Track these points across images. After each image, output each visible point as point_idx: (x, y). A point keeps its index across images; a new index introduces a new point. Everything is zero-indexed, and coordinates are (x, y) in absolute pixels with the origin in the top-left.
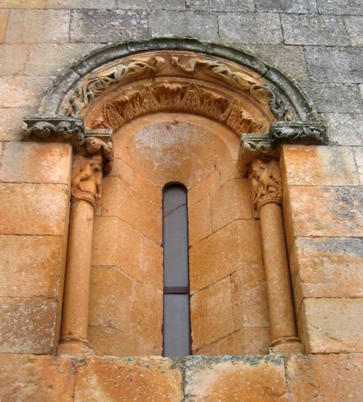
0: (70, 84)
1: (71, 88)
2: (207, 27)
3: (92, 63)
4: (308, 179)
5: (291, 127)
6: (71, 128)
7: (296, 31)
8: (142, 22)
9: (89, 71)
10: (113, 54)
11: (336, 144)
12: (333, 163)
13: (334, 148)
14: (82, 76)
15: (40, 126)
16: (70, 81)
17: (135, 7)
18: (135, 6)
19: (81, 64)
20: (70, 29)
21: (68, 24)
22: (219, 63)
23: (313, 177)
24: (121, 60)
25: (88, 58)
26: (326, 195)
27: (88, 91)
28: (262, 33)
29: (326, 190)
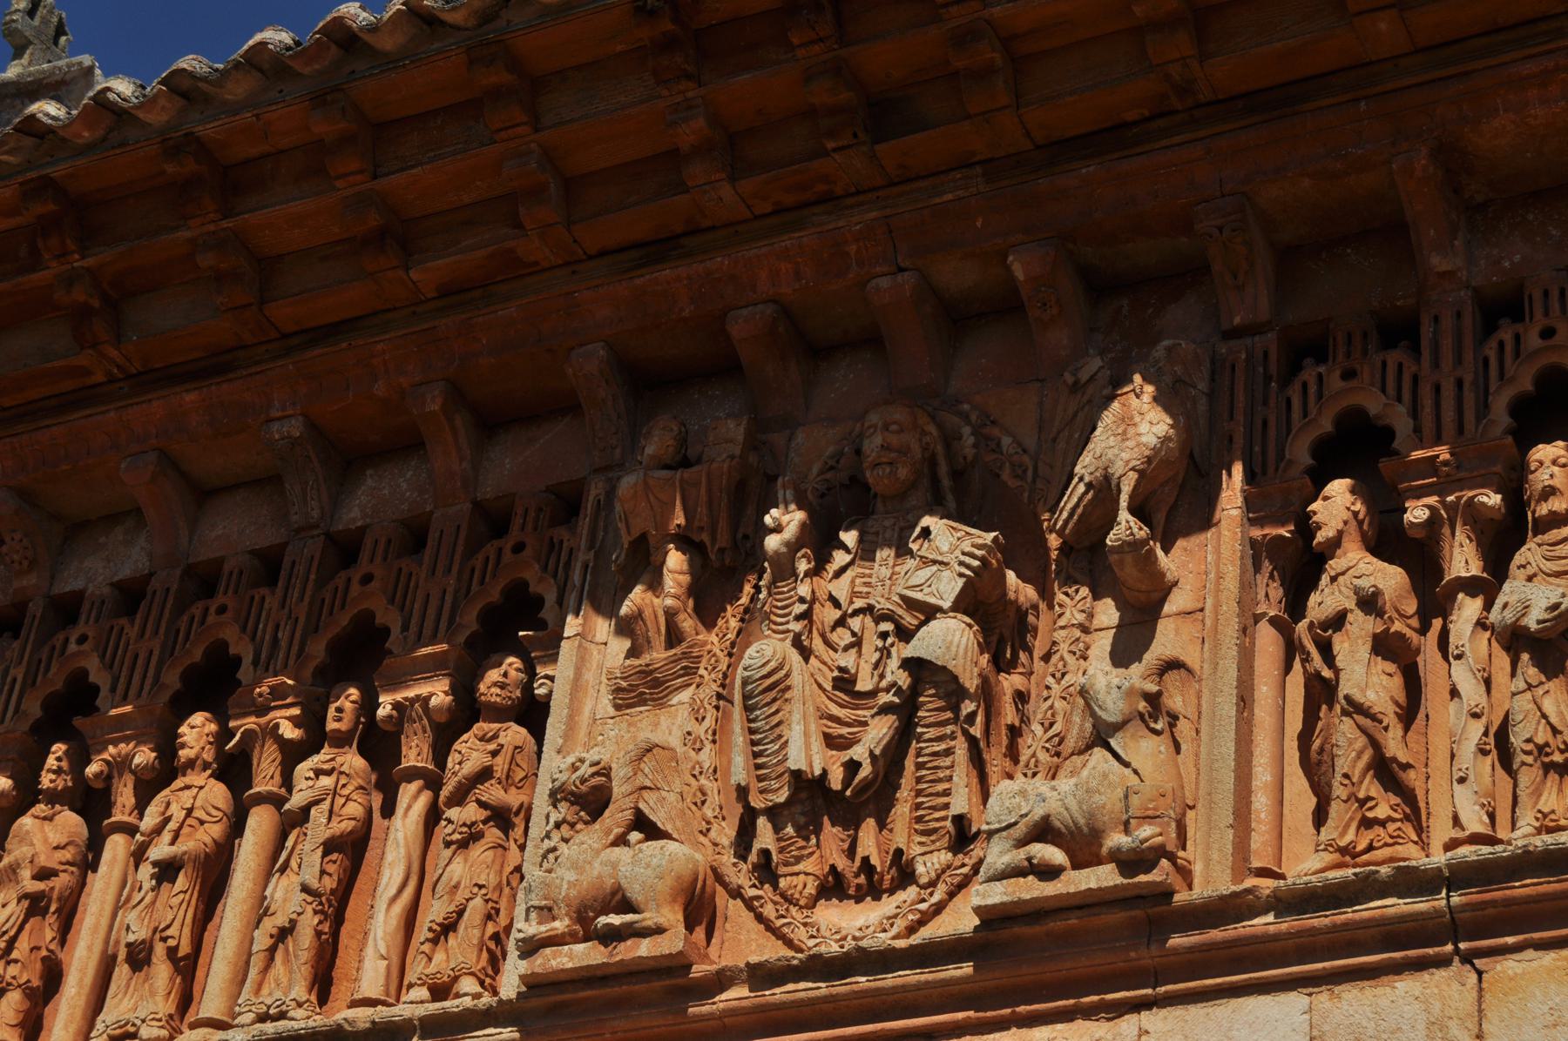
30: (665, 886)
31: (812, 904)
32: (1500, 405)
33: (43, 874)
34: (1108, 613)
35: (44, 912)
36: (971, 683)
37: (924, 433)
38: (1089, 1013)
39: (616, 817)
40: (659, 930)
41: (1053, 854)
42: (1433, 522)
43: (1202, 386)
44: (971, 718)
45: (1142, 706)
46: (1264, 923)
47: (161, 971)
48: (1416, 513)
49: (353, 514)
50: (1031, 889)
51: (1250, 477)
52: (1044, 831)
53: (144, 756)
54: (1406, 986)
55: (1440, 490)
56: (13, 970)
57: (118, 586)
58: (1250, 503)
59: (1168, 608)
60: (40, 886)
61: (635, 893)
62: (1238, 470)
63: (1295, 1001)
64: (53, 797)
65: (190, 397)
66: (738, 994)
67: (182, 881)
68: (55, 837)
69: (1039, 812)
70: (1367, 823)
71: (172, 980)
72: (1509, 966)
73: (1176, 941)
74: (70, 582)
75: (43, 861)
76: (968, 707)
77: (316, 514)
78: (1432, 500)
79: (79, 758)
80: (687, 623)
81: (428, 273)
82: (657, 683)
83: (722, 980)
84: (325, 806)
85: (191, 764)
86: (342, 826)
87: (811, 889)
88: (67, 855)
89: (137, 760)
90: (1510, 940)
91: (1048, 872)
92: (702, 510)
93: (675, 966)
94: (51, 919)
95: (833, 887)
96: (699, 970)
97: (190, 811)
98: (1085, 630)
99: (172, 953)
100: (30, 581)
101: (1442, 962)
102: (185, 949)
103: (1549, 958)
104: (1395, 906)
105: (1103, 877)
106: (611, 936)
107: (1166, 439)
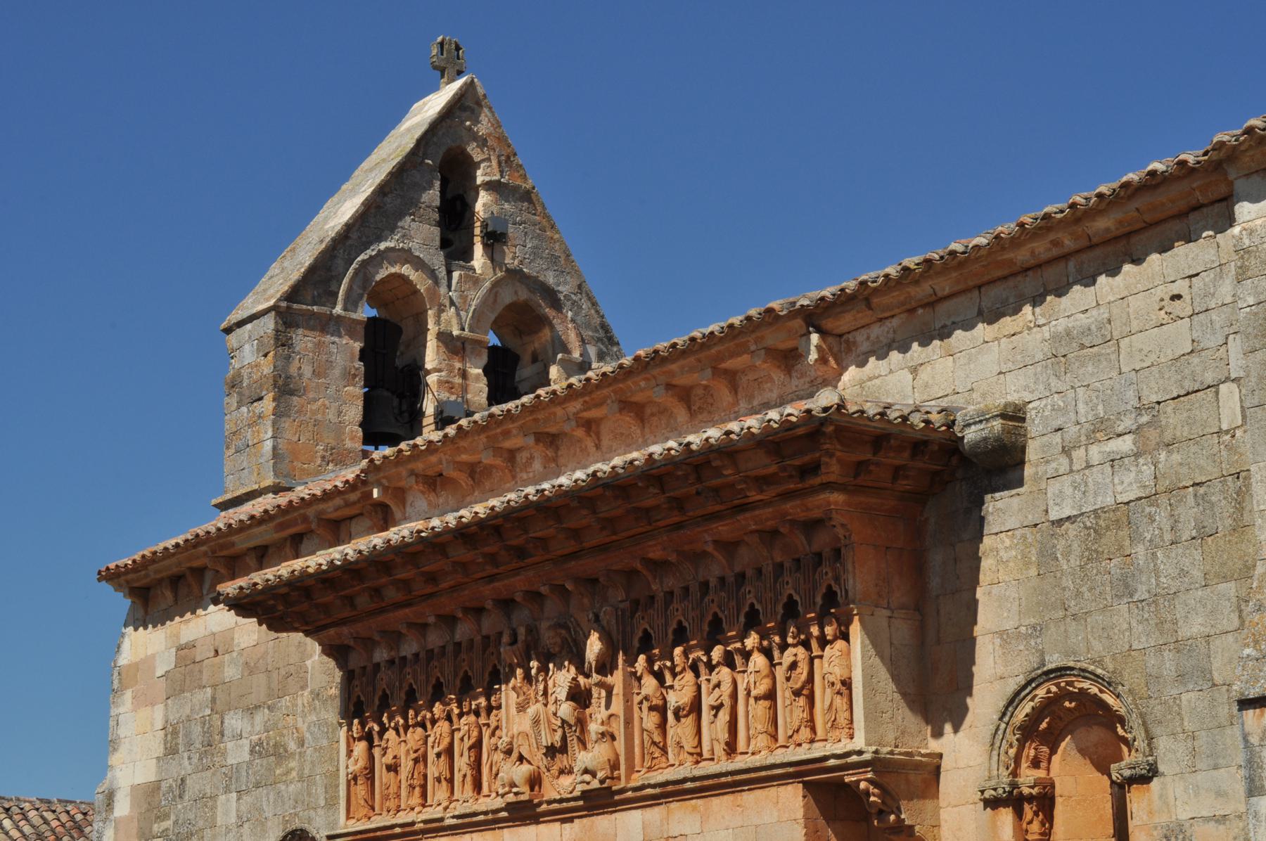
0: (1001, 737)
1: (1002, 739)
2: (1080, 638)
3: (1010, 709)
4: (1145, 818)
5: (1129, 768)
6: (1005, 792)
7: (1140, 628)
8: (1039, 640)
9: (1011, 716)
10: (1023, 694)
11: (1163, 774)
12: (1161, 796)
13: (1162, 779)
14: (1007, 724)
15: (987, 795)
16: (1000, 732)
17: (1033, 621)
18: (1032, 619)
19: (1004, 714)
20: (995, 663)
21: (992, 655)
22: (1091, 684)
23: (1148, 816)
24: (1029, 697)
25: (1007, 708)
26: (1155, 833)
27: (1014, 735)
28: (1116, 637)
29: (1156, 828)
30: (523, 781)
31: (558, 777)
32: (670, 631)
33: (416, 751)
34: (603, 693)
35: (419, 761)
36: (572, 722)
37: (561, 634)
38: (607, 813)
39: (515, 755)
40: (523, 793)
41: (587, 777)
42: (660, 667)
43: (614, 621)
44: (575, 731)
45: (600, 736)
46: (630, 794)
47: (444, 783)
48: (656, 668)
49: (458, 638)
50: (586, 787)
51: (625, 654)
52: (586, 771)
53: (429, 715)
54: (657, 809)
55: (660, 659)
56: (415, 781)
57: (413, 654)
58: (625, 661)
59: (614, 692)
60: (416, 755)
61: (517, 783)
62: (621, 652)
63: (639, 811)
64: (414, 726)
65: (407, 610)
66: (544, 807)
67: (443, 758)
68: (417, 738)
69: (584, 767)
70: (654, 758)
71: (447, 786)
72: (673, 805)
73: (617, 798)
74: (403, 654)
75: (414, 748)
76: (574, 728)
77: (448, 638)
78: (658, 663)
79: (416, 716)
80: (525, 689)
81: (444, 585)
82: (522, 707)
83: (540, 804)
84: (467, 736)
85: (439, 719)
86: (473, 740)
87: (557, 774)
88: (421, 742)
89: (427, 717)
90: (671, 799)
91: (588, 783)
92: (519, 658)
93: (530, 801)
94: (422, 763)
95: (562, 772)
96: (536, 801)
97: (441, 735)
98: (599, 698)
99: (445, 778)
100: (393, 653)
101: (661, 804)
102: (448, 776)
103: (678, 803)
104: (649, 791)
105: (595, 784)
106: (516, 794)
107: (601, 649)
